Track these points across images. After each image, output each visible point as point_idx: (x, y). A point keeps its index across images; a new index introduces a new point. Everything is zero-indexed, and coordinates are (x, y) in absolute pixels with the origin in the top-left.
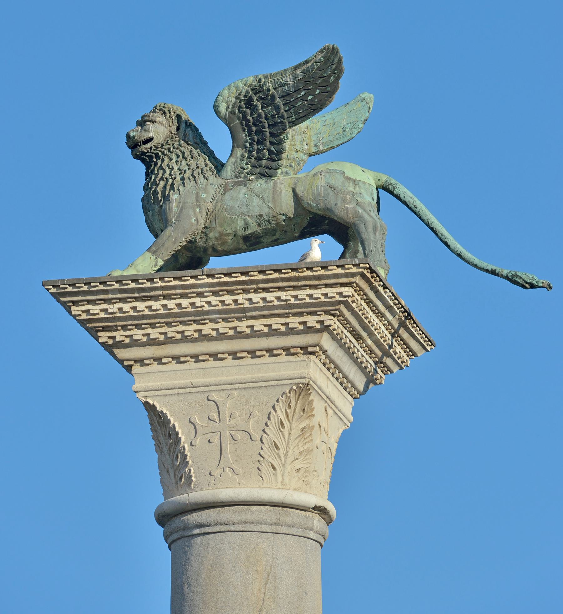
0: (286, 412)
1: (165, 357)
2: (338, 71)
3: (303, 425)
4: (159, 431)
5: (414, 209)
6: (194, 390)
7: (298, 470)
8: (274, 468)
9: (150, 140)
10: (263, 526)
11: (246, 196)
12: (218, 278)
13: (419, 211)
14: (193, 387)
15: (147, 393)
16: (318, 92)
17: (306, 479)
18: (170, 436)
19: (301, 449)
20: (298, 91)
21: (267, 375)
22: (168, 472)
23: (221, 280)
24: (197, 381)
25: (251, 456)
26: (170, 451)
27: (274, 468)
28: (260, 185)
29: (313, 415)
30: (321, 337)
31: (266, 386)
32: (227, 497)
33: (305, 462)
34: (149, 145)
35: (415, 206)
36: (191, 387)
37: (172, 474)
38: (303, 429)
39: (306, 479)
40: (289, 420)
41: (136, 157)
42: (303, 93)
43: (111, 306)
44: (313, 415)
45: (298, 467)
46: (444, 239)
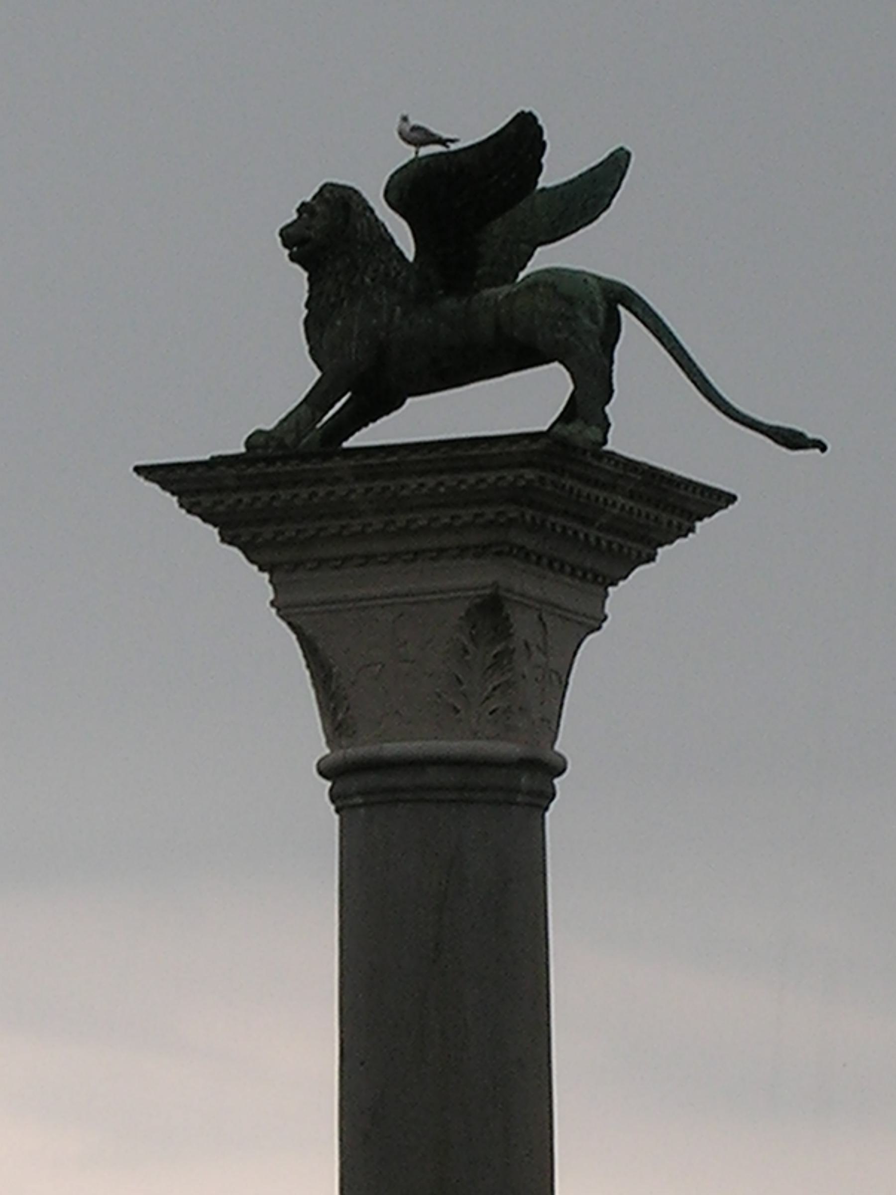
8: (457, 711)
11: (430, 321)
18: (322, 666)
28: (450, 304)
29: (511, 635)
42: (496, 177)
44: (511, 635)
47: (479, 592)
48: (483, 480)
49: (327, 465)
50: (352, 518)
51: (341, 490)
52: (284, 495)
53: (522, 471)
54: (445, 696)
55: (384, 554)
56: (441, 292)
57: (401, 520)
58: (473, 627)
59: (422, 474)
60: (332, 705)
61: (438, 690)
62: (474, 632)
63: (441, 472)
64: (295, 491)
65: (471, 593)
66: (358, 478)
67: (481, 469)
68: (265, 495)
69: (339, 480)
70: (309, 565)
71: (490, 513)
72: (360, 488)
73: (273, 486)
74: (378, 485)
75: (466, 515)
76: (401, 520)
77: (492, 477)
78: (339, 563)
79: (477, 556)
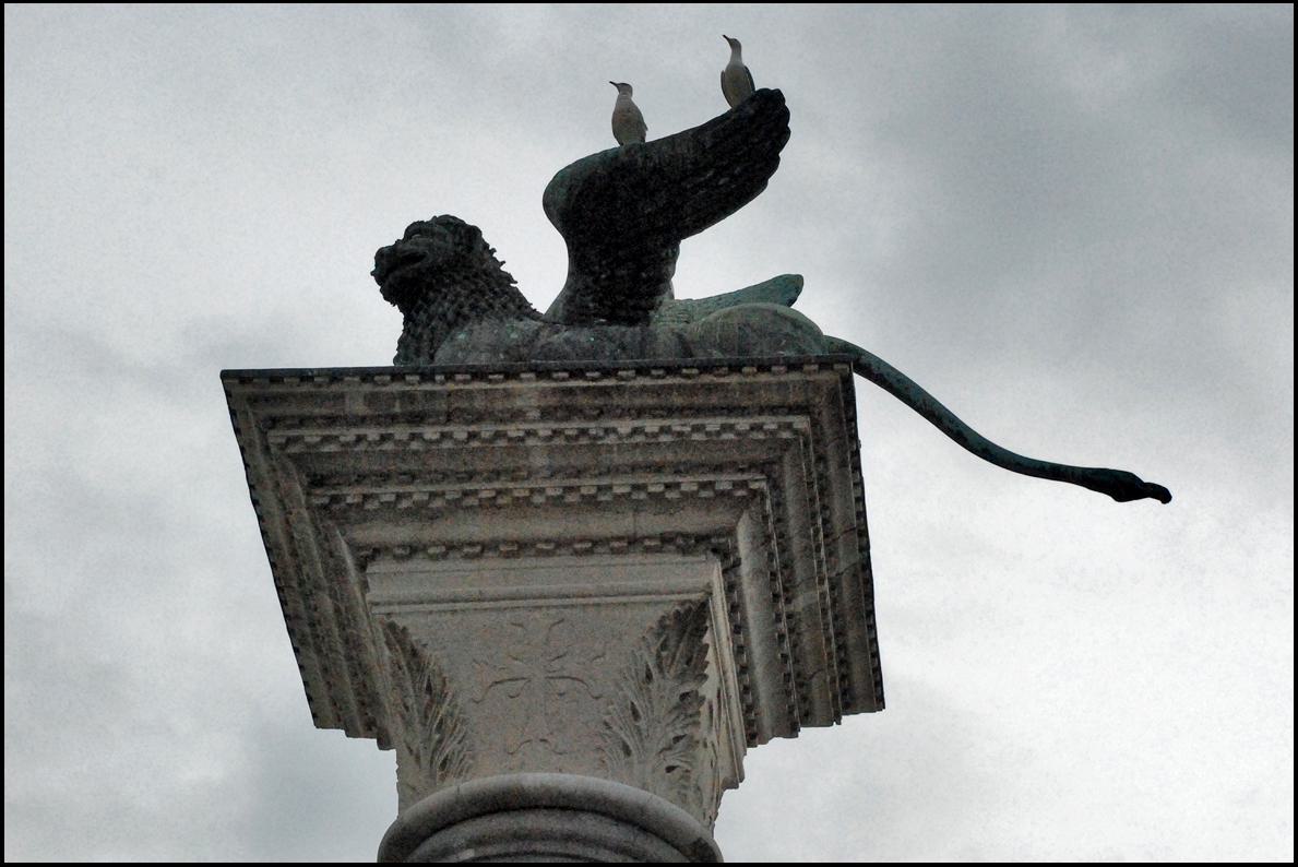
0: (659, 656)
1: (434, 544)
2: (781, 134)
3: (686, 688)
4: (408, 684)
5: (896, 385)
6: (486, 605)
7: (670, 769)
8: (627, 752)
9: (421, 257)
10: (602, 851)
12: (556, 380)
13: (906, 388)
14: (484, 601)
15: (396, 608)
16: (738, 170)
17: (683, 791)
18: (429, 689)
19: (680, 733)
20: (698, 170)
21: (630, 583)
22: (418, 758)
23: (564, 384)
24: (490, 590)
25: (586, 724)
26: (426, 717)
27: (627, 752)
30: (739, 517)
31: (625, 604)
32: (538, 785)
33: (684, 759)
34: (417, 265)
35: (898, 381)
36: (479, 600)
37: (424, 761)
38: (684, 696)
39: (683, 791)
40: (661, 670)
41: (391, 294)
43: (345, 431)
45: (672, 763)
46: (955, 429)
47: (685, 597)
48: (731, 428)
49: (511, 385)
50: (514, 480)
51: (514, 430)
52: (431, 433)
53: (790, 419)
54: (615, 728)
55: (547, 541)
56: (603, 320)
57: (588, 485)
58: (664, 646)
59: (640, 412)
60: (437, 737)
61: (607, 718)
62: (664, 654)
63: (671, 411)
64: (446, 429)
65: (674, 597)
66: (546, 414)
67: (730, 410)
68: (401, 432)
69: (517, 415)
70: (432, 551)
71: (724, 482)
72: (544, 429)
73: (417, 419)
74: (571, 428)
75: (688, 483)
76: (588, 485)
77: (743, 424)
78: (478, 549)
79: (684, 551)
